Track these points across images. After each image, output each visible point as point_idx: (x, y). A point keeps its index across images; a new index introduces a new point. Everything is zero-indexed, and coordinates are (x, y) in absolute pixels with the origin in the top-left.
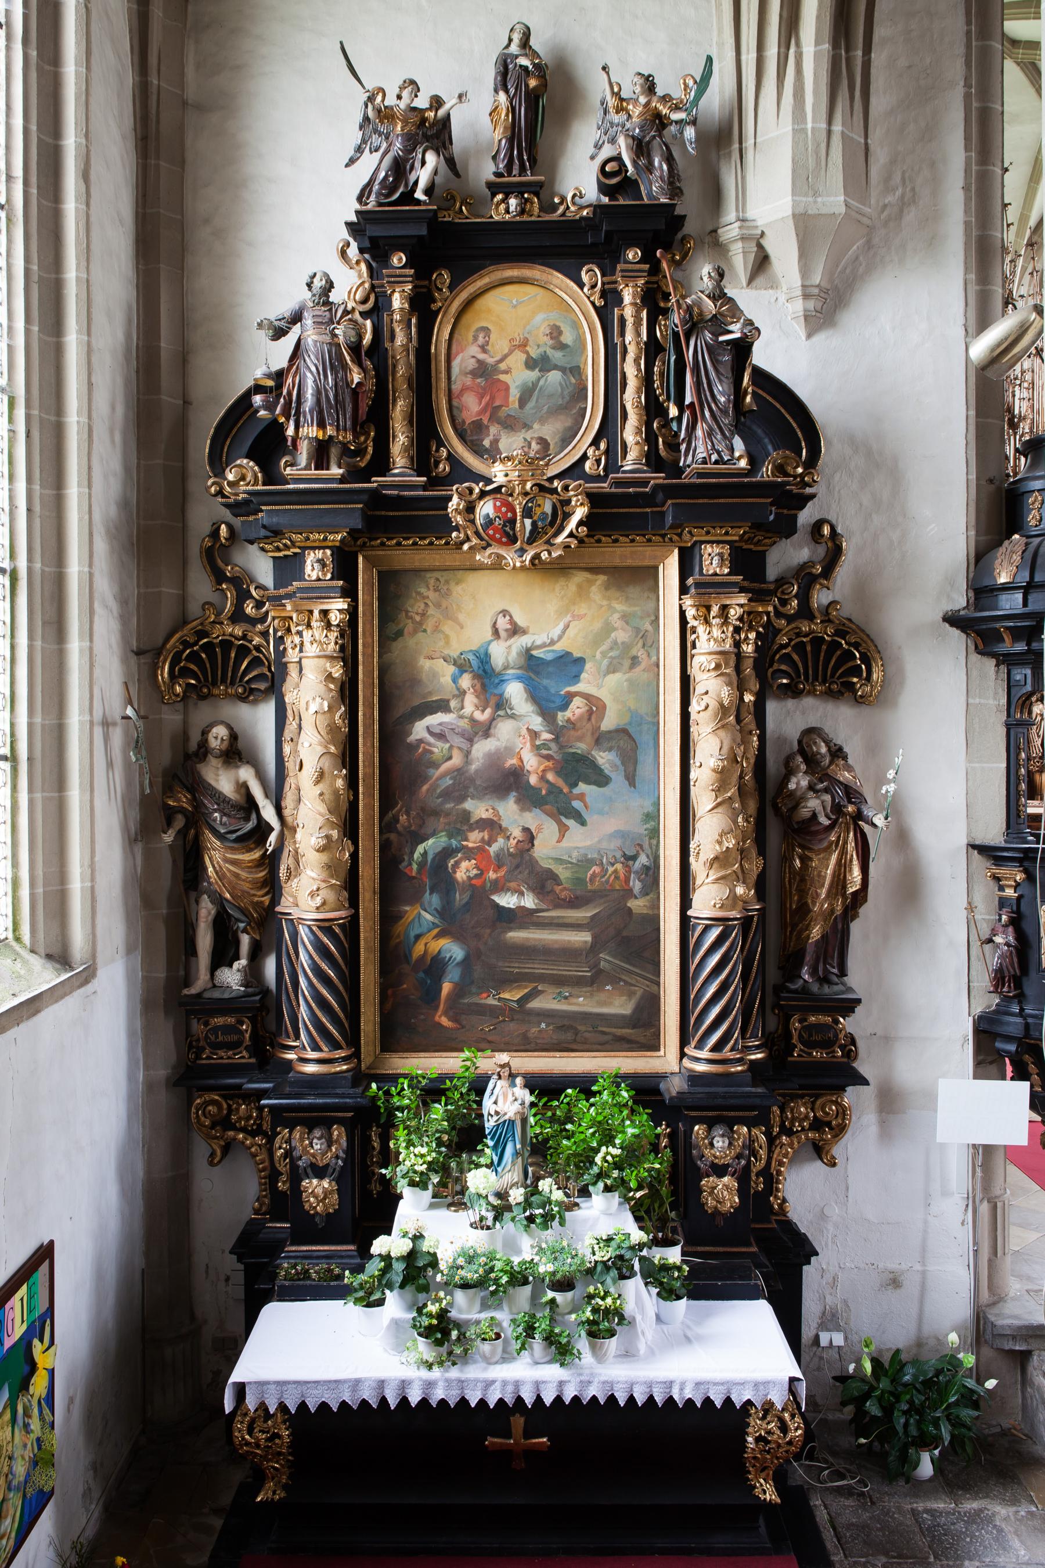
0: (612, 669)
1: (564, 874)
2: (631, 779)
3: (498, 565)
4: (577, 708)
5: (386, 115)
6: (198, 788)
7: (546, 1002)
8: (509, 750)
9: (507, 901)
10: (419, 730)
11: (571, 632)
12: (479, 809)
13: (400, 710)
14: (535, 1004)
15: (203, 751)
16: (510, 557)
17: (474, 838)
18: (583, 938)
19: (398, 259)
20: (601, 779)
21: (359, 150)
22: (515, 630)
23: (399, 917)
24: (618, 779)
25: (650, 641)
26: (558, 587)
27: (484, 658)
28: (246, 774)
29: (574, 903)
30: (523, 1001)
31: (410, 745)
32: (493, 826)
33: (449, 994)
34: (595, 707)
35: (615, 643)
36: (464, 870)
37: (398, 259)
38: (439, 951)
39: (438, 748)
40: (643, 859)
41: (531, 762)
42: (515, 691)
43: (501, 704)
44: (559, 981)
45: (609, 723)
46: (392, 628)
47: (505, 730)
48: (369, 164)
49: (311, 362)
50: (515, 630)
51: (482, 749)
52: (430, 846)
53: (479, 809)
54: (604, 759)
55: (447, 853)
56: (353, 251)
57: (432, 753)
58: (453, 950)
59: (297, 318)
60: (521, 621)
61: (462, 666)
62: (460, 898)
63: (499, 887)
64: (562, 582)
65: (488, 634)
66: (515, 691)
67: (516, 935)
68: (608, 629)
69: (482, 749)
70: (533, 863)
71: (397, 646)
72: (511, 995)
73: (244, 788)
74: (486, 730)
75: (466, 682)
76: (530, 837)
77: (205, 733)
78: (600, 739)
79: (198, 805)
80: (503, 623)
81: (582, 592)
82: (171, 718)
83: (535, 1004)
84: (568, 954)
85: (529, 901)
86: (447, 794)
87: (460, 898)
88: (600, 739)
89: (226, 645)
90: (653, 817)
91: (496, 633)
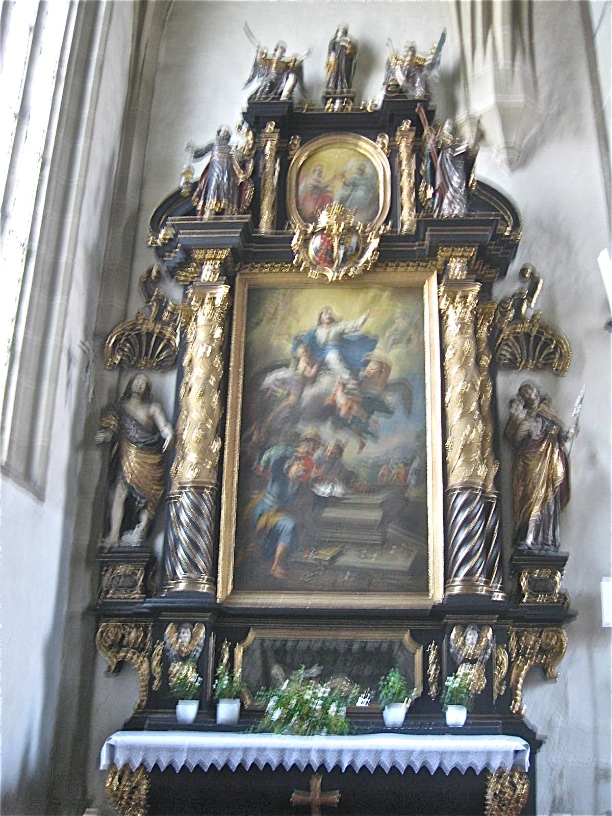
0: (396, 342)
1: (363, 473)
2: (408, 410)
3: (322, 282)
4: (372, 367)
5: (267, 62)
6: (122, 415)
7: (350, 559)
8: (327, 393)
9: (324, 490)
10: (270, 380)
11: (370, 320)
12: (308, 430)
13: (257, 367)
14: (342, 561)
15: (128, 394)
16: (330, 274)
17: (302, 449)
18: (375, 515)
19: (270, 127)
20: (387, 411)
21: (253, 77)
22: (332, 321)
23: (249, 500)
24: (399, 413)
25: (419, 326)
26: (361, 294)
27: (313, 337)
28: (155, 410)
29: (371, 491)
30: (333, 559)
31: (262, 392)
32: (316, 441)
33: (280, 555)
34: (384, 367)
35: (396, 330)
36: (295, 470)
37: (270, 127)
38: (275, 526)
39: (281, 392)
40: (415, 465)
41: (341, 400)
42: (332, 357)
43: (323, 367)
44: (359, 545)
45: (394, 375)
46: (255, 320)
47: (325, 381)
48: (256, 84)
49: (216, 172)
50: (332, 321)
51: (310, 392)
52: (273, 454)
53: (308, 430)
54: (391, 399)
55: (283, 459)
56: (245, 128)
57: (276, 396)
58: (286, 523)
59: (210, 148)
60: (337, 313)
61: (298, 341)
62: (291, 489)
63: (319, 480)
64: (362, 295)
65: (316, 322)
66: (332, 357)
67: (330, 513)
68: (391, 322)
69: (310, 392)
70: (342, 466)
71: (257, 333)
72: (326, 554)
73: (152, 418)
74: (314, 380)
75: (301, 350)
76: (339, 449)
77: (131, 383)
78: (387, 387)
79: (121, 427)
80: (325, 317)
81: (375, 300)
82: (111, 378)
83: (342, 561)
84: (365, 526)
85: (338, 490)
86: (286, 420)
87: (291, 489)
88: (387, 387)
89: (150, 335)
90: (422, 436)
91: (320, 323)
